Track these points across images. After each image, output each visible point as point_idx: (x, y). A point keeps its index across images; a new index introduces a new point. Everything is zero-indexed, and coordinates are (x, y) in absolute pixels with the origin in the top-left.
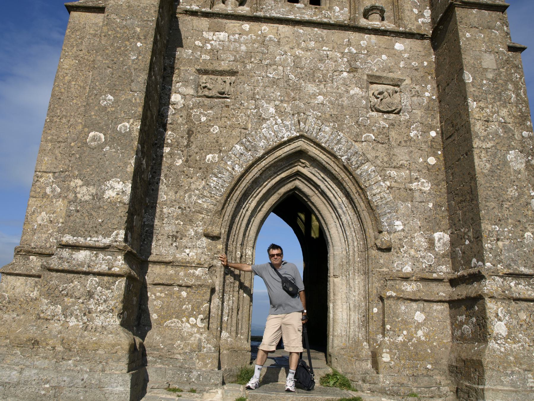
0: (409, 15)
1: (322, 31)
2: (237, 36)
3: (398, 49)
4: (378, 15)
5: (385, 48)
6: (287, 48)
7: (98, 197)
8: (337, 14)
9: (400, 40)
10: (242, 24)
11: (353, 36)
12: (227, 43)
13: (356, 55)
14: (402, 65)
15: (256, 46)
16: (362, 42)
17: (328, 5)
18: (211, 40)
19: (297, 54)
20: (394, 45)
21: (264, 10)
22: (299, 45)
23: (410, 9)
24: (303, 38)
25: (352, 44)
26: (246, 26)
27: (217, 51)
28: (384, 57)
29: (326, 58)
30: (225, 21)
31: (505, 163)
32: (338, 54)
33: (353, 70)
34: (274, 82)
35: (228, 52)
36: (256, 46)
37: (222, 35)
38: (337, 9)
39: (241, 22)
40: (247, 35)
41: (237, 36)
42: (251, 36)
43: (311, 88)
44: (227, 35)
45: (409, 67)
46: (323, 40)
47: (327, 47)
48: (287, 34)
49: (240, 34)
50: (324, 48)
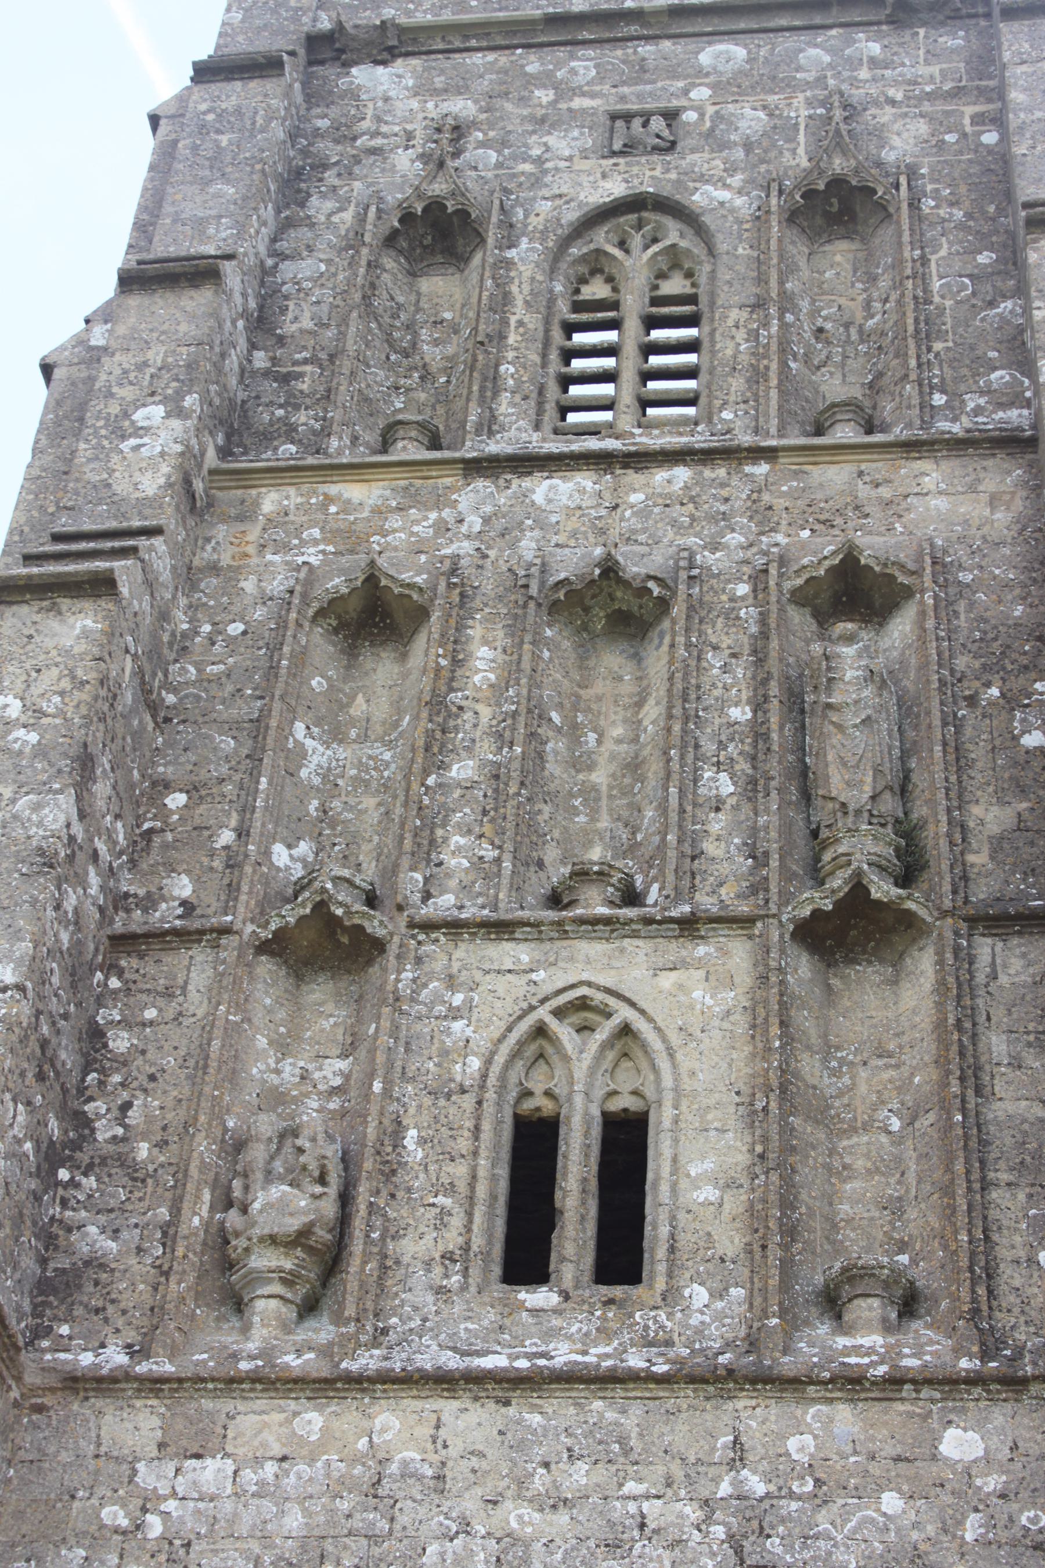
0: (1017, 1283)
1: (624, 1412)
2: (270, 1469)
3: (955, 1455)
4: (876, 1303)
5: (898, 1459)
6: (470, 1504)
8: (695, 1320)
9: (964, 1410)
10: (296, 1414)
11: (755, 1416)
12: (228, 1506)
13: (766, 1504)
14: (972, 1529)
15: (344, 1506)
16: (793, 1444)
17: (660, 1284)
18: (165, 1498)
19: (514, 1524)
20: (936, 1440)
21: (392, 1337)
22: (522, 1483)
23: (1022, 1254)
24: (539, 1452)
25: (750, 1457)
26: (312, 1421)
27: (188, 1545)
28: (891, 1502)
29: (636, 1533)
30: (227, 1405)
32: (688, 1510)
35: (228, 1543)
36: (344, 1506)
37: (211, 1471)
38: (699, 1295)
39: (292, 1405)
40: (312, 1461)
41: (270, 1469)
42: (328, 1463)
44: (229, 1466)
45: (1004, 1535)
46: (627, 1451)
47: (640, 1480)
48: (477, 1440)
49: (284, 1459)
50: (631, 1487)
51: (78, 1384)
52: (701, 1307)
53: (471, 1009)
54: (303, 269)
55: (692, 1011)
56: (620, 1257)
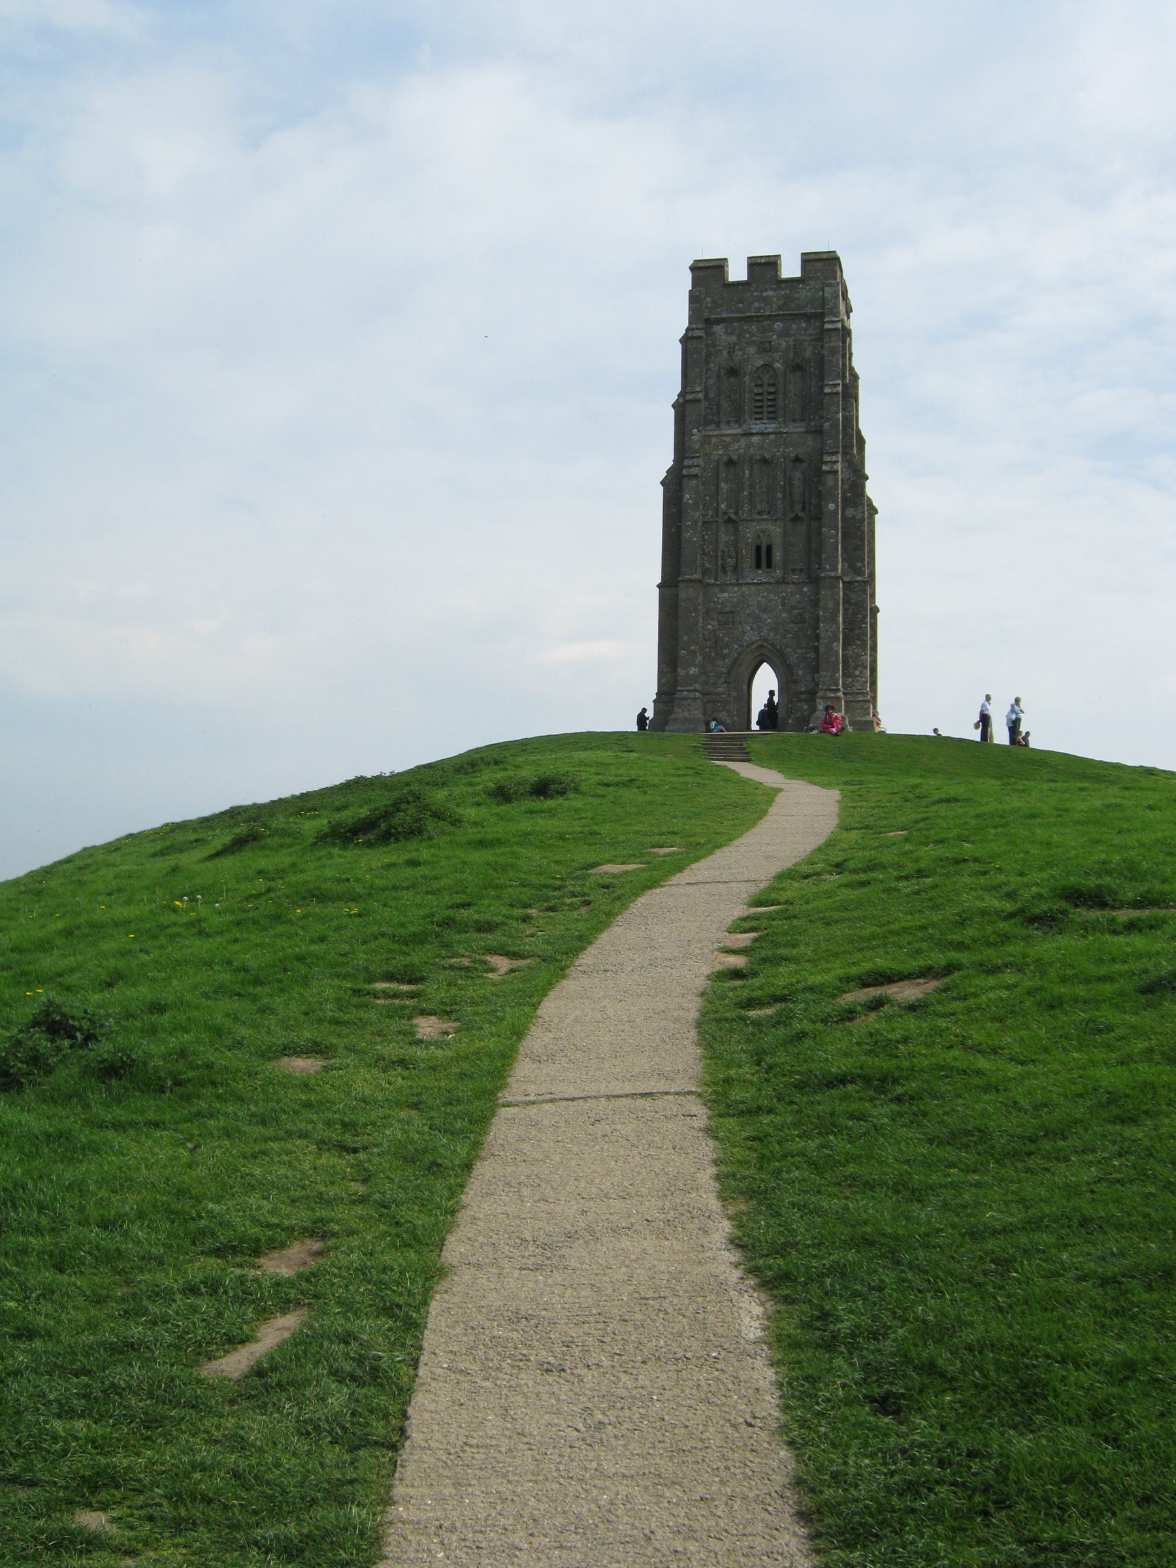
7: (687, 674)
11: (784, 587)
31: (831, 648)
33: (784, 604)
34: (749, 615)
43: (765, 616)
51: (708, 584)
52: (779, 573)
53: (749, 533)
54: (712, 381)
55: (775, 530)
56: (769, 565)
